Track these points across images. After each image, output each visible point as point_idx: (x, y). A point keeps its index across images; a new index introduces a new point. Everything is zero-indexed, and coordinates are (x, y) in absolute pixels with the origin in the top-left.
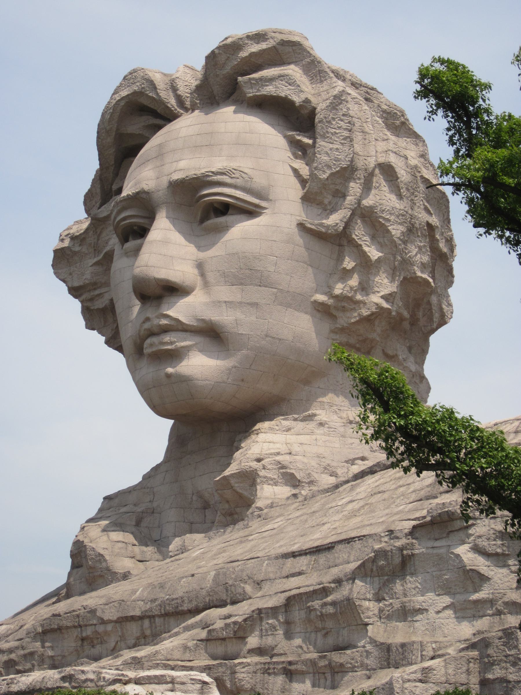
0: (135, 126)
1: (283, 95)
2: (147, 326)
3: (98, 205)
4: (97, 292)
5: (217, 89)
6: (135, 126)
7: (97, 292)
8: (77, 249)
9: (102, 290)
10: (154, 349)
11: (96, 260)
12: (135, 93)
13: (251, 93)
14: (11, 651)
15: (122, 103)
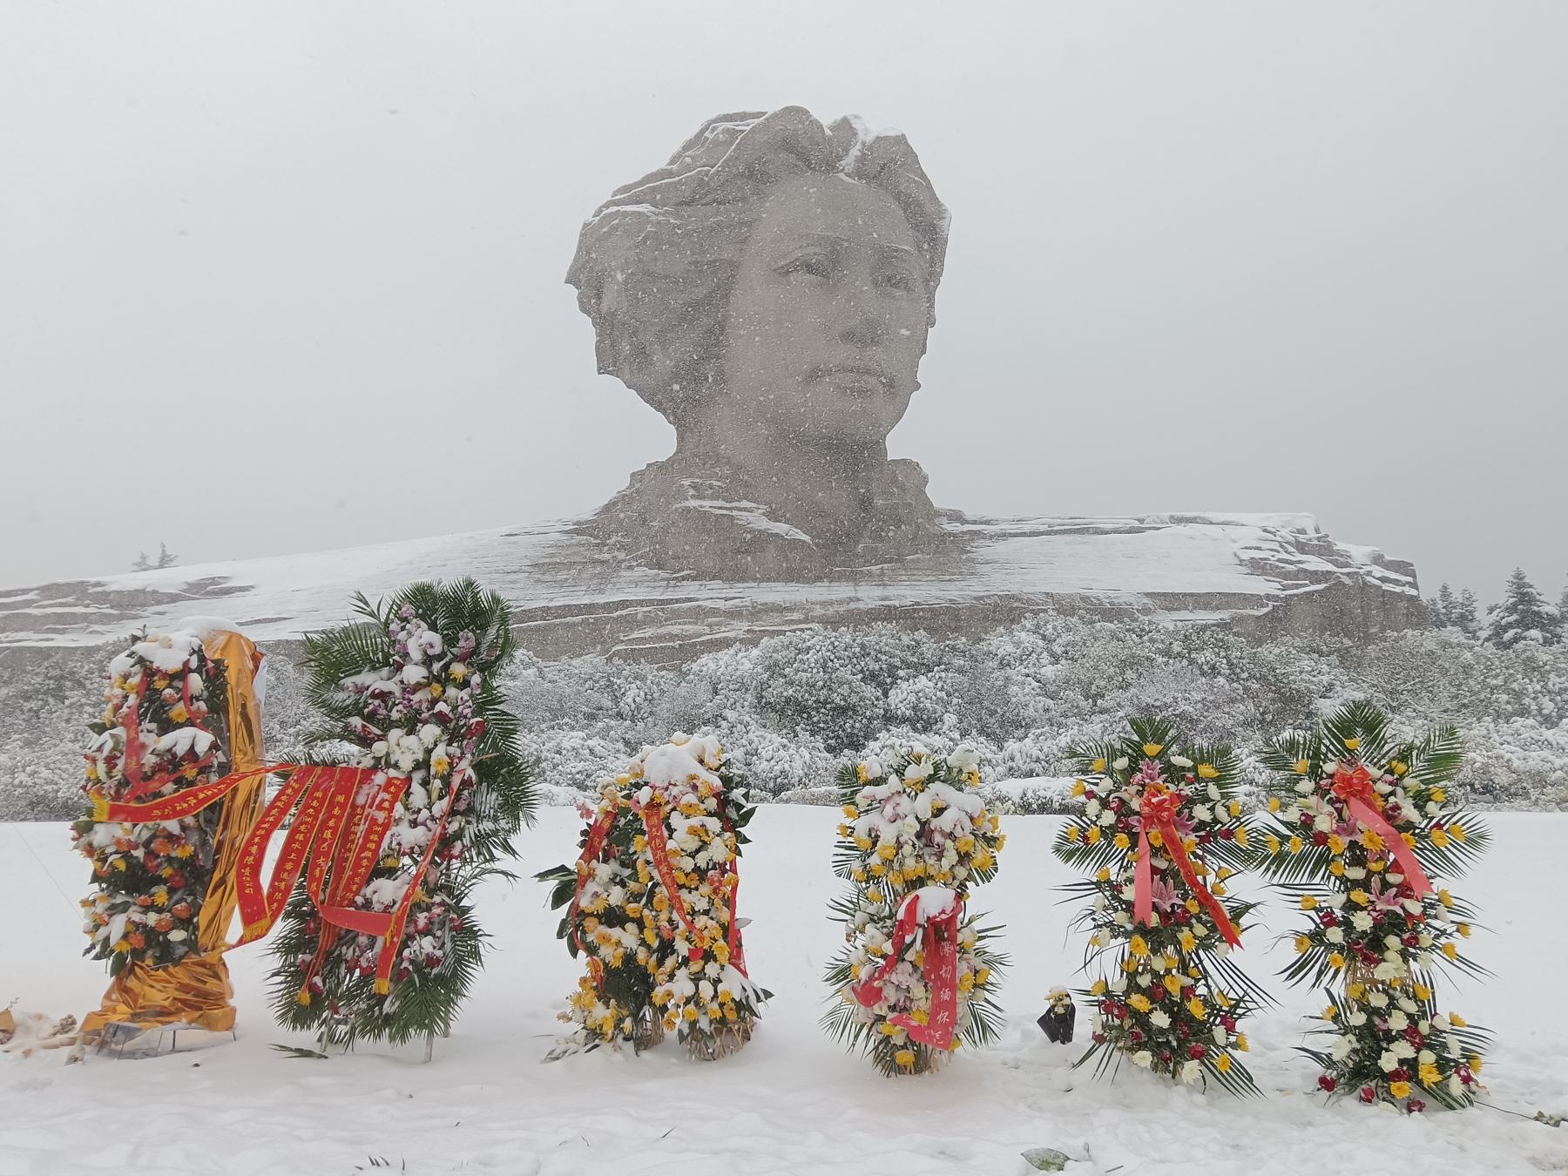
5: (873, 169)
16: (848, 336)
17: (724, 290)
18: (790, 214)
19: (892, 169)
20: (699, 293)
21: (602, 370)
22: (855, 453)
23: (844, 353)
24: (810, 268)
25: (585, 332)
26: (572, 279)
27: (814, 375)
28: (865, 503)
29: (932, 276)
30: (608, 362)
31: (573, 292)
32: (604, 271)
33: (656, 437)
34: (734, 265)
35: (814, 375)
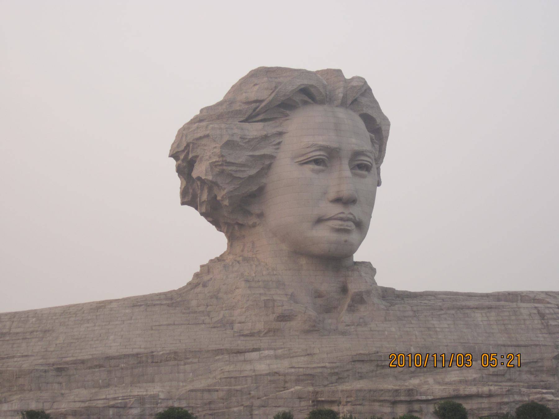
0: (298, 98)
1: (374, 116)
2: (341, 215)
3: (242, 119)
4: (243, 169)
5: (349, 102)
6: (298, 98)
7: (243, 169)
8: (241, 144)
9: (246, 169)
10: (342, 227)
11: (251, 153)
12: (312, 86)
13: (365, 111)
14: (332, 368)
15: (302, 87)
16: (338, 200)
17: (266, 170)
18: (304, 130)
19: (357, 99)
20: (253, 172)
21: (183, 204)
22: (337, 261)
23: (335, 210)
24: (317, 162)
25: (176, 183)
26: (174, 155)
27: (320, 221)
28: (344, 290)
29: (379, 159)
30: (189, 198)
31: (173, 163)
32: (197, 157)
33: (213, 242)
34: (272, 157)
35: (320, 221)
